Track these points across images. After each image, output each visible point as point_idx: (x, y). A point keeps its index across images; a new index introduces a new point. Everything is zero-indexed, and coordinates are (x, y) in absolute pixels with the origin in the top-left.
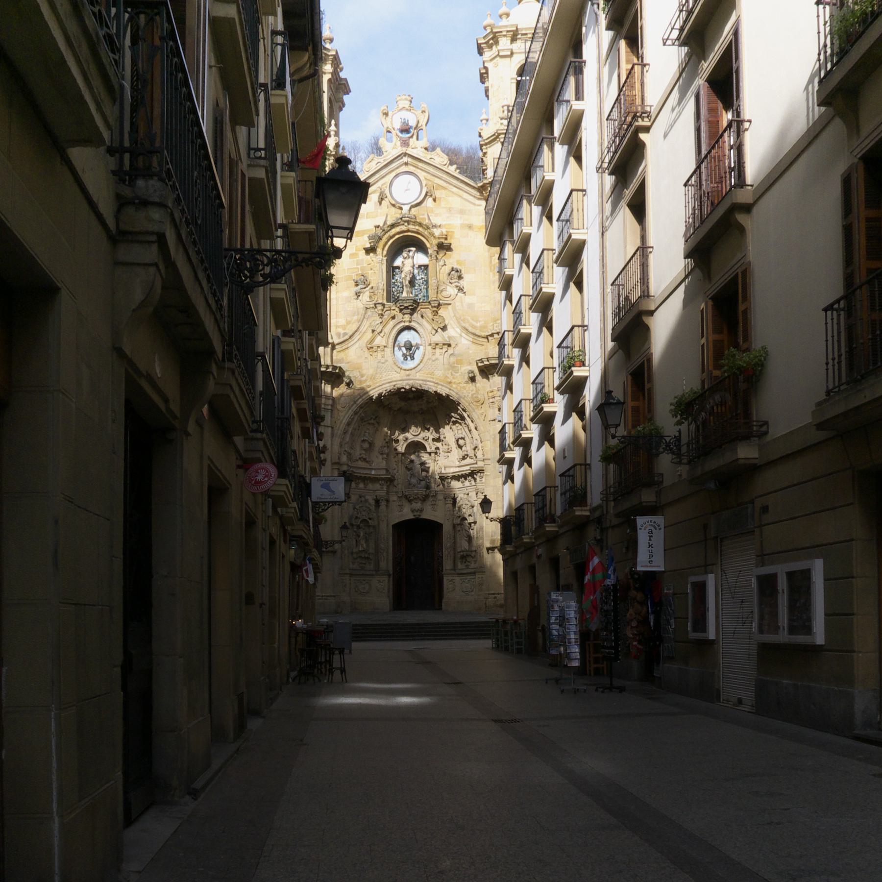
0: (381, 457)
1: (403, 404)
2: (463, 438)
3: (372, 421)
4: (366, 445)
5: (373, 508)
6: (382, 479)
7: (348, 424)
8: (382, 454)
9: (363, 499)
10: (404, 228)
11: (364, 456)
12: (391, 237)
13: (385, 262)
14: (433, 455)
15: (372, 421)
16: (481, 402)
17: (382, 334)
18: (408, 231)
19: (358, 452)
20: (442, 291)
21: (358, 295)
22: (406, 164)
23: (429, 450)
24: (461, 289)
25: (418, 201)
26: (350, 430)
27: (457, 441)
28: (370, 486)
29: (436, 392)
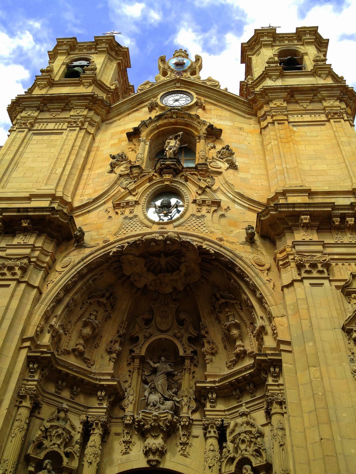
0: (107, 357)
1: (151, 277)
2: (237, 326)
3: (104, 300)
4: (87, 331)
5: (77, 437)
6: (102, 388)
7: (67, 289)
8: (110, 352)
9: (62, 415)
10: (172, 120)
11: (81, 348)
12: (158, 127)
13: (148, 143)
14: (187, 362)
15: (104, 300)
16: (267, 266)
17: (134, 193)
18: (176, 123)
19: (72, 341)
20: (211, 162)
21: (113, 166)
22: (178, 87)
23: (181, 353)
24: (233, 166)
25: (189, 105)
26: (67, 300)
27: (229, 329)
28: (81, 399)
29: (200, 247)
